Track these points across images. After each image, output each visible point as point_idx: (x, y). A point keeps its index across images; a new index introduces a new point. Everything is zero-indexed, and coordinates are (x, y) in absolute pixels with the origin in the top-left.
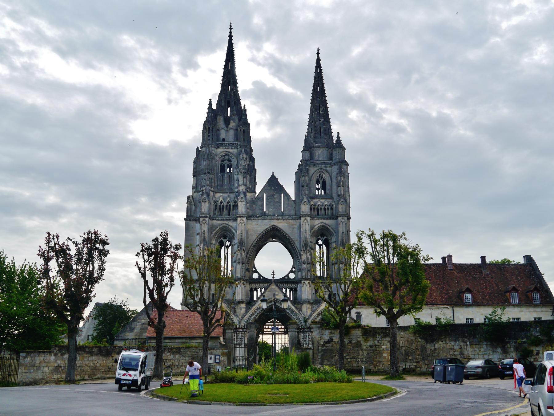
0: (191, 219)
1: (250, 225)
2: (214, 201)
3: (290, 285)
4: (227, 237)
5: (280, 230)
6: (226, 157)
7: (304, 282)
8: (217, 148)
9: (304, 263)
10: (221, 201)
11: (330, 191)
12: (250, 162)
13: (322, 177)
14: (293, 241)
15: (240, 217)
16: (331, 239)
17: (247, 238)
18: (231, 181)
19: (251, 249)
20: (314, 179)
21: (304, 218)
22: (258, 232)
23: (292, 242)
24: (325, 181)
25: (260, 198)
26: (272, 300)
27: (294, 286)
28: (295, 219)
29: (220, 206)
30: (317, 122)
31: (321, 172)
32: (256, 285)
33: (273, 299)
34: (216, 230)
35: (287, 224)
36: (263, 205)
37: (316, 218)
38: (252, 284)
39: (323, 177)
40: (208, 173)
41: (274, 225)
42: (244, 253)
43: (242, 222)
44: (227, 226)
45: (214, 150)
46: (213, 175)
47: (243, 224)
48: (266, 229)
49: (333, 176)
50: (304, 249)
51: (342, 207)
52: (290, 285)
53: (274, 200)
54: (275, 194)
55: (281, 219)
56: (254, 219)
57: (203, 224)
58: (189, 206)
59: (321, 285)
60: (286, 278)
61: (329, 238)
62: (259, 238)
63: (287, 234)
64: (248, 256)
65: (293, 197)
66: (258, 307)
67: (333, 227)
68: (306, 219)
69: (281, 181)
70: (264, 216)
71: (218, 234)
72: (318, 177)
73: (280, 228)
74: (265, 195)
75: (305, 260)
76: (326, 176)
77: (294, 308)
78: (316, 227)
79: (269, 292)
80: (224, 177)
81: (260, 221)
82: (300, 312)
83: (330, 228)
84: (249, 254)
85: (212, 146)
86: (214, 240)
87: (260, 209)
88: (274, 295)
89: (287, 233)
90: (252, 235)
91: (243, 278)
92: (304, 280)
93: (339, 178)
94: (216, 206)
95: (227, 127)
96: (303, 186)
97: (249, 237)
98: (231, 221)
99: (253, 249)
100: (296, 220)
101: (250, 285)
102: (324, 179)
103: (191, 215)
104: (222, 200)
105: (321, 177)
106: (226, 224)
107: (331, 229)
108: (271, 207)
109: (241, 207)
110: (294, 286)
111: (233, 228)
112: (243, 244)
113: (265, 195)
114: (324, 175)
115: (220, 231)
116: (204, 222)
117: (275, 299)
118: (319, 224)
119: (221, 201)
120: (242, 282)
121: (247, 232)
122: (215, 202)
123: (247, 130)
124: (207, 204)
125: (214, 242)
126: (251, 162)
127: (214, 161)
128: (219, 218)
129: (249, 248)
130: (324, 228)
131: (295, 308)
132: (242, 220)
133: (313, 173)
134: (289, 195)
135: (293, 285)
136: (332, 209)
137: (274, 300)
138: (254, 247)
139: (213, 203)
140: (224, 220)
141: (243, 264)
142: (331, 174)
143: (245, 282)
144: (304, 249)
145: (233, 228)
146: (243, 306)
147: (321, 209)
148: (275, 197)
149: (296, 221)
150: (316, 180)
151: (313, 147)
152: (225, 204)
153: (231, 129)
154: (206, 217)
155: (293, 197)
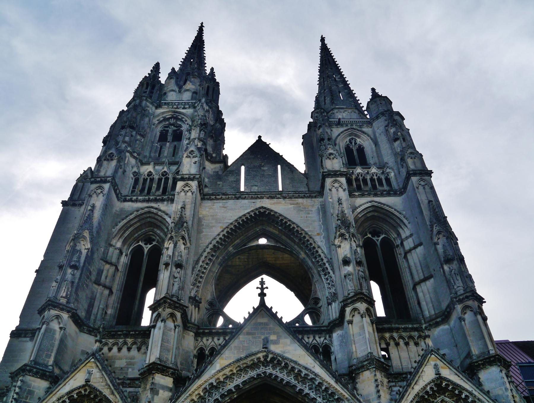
0: (77, 203)
1: (207, 209)
2: (135, 172)
3: (311, 339)
4: (154, 240)
5: (277, 215)
6: (172, 121)
7: (355, 309)
8: (156, 108)
9: (346, 262)
10: (150, 172)
11: (376, 159)
12: (216, 123)
13: (355, 143)
14: (309, 235)
15: (182, 179)
16: (399, 235)
17: (199, 232)
18: (178, 153)
19: (205, 254)
20: (341, 145)
21: (333, 179)
22: (225, 222)
23: (307, 238)
24: (363, 148)
25: (233, 171)
26: (259, 358)
27: (320, 340)
28: (310, 197)
29: (145, 180)
30: (333, 88)
31: (350, 135)
32: (216, 339)
33: (260, 355)
34: (128, 219)
35: (293, 205)
36: (239, 181)
37: (357, 194)
38: (204, 339)
39: (358, 143)
40: (132, 127)
41: (262, 207)
42: (183, 247)
43: (187, 189)
44: (155, 211)
45: (151, 109)
46: (140, 135)
47: (189, 194)
48: (244, 215)
49: (377, 135)
50: (343, 231)
51: (414, 163)
52: (311, 339)
53: (262, 173)
54: (265, 164)
55: (279, 196)
56: (217, 197)
57: (95, 195)
58: (80, 184)
59: (395, 335)
60: (297, 325)
61: (394, 235)
62: (227, 232)
63: (294, 223)
64: (198, 268)
65: (301, 167)
66: (213, 381)
67: (400, 207)
68: (336, 181)
69: (276, 147)
70: (239, 196)
71: (130, 229)
72: (348, 142)
73: (276, 213)
74: (243, 168)
75: (349, 256)
76: (364, 141)
77: (332, 382)
78: (359, 210)
79: (248, 334)
80: (164, 147)
81: (231, 202)
82: (355, 397)
83: (392, 210)
84: (201, 263)
85: (146, 100)
86: (121, 240)
87: (233, 188)
88: (266, 343)
89: (294, 221)
90: (212, 227)
91: (175, 299)
92: (353, 302)
93: (392, 130)
94: (136, 181)
95: (180, 88)
96: (323, 140)
97: (204, 230)
98: (165, 203)
99: (212, 256)
100: (312, 197)
101: (197, 340)
102: (360, 146)
103: (79, 198)
104: (152, 171)
105: (353, 144)
106: (152, 207)
107: (397, 214)
108: (257, 185)
109: (188, 166)
110: (320, 340)
111: (167, 214)
112: (182, 226)
113: (243, 168)
114: (358, 141)
115: (138, 224)
116: (99, 191)
117: (270, 356)
118: (365, 203)
119: (150, 172)
120: (169, 311)
121: (200, 220)
122: (136, 175)
123: (214, 89)
124: (114, 163)
125: (119, 245)
126: (218, 124)
127: (147, 119)
128: (140, 198)
129: (200, 251)
130: (376, 214)
131: (336, 382)
132: (187, 185)
133: (339, 135)
134: (293, 166)
135: (317, 338)
136: (388, 180)
137: (266, 357)
138: (215, 249)
139: (132, 176)
140: (148, 201)
141: (179, 266)
142: (372, 137)
143: (178, 315)
144: (343, 231)
145: (167, 214)
146: (168, 381)
147: (365, 181)
148: (265, 168)
149: (313, 199)
150: (344, 146)
151: (332, 110)
152: (156, 177)
153: (188, 90)
154: (105, 182)
155: (301, 167)
